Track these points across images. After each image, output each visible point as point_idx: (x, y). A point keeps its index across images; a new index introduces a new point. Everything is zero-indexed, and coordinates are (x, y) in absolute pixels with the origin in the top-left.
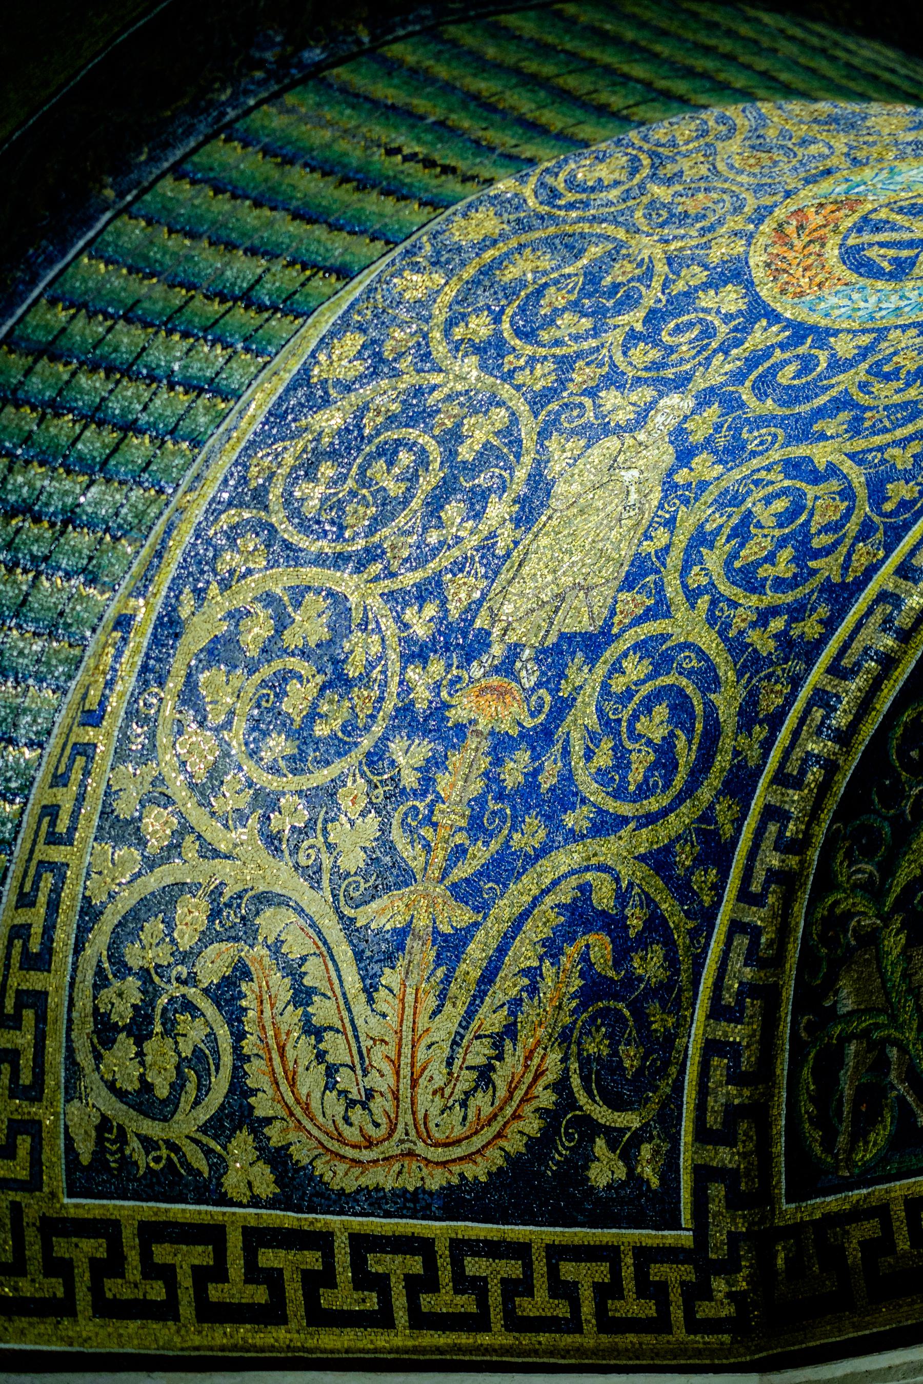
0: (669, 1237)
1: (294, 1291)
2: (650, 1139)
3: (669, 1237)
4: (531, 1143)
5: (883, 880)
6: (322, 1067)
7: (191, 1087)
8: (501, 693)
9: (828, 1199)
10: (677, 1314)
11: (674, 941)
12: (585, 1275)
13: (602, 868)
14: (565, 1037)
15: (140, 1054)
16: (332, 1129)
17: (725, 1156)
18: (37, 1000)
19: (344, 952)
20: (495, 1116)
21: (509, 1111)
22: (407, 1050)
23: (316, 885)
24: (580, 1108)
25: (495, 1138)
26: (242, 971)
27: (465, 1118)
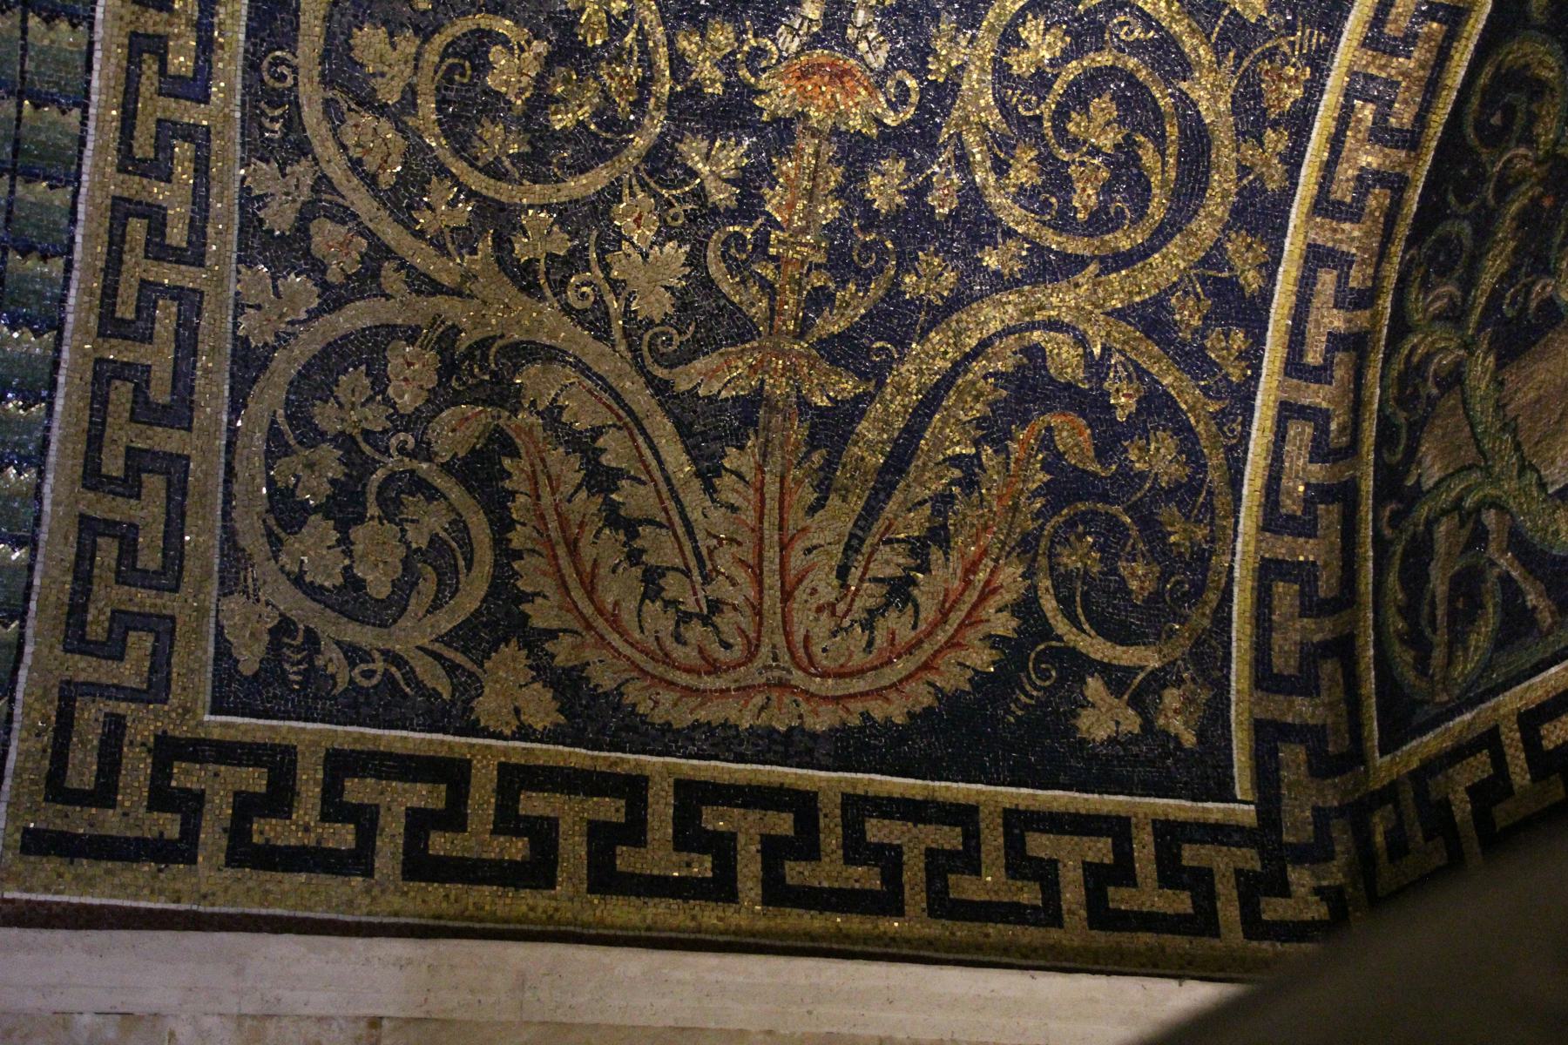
0: (1214, 810)
1: (573, 848)
2: (1180, 682)
3: (1214, 810)
4: (980, 680)
5: (1464, 300)
6: (637, 571)
7: (428, 587)
8: (840, 75)
9: (1425, 739)
10: (1229, 911)
11: (1191, 429)
12: (1073, 857)
13: (1053, 325)
14: (1027, 545)
15: (345, 541)
16: (654, 646)
17: (1302, 709)
18: (175, 467)
19: (663, 428)
20: (919, 643)
21: (941, 637)
22: (772, 554)
23: (603, 335)
24: (1059, 638)
25: (919, 669)
26: (502, 443)
27: (870, 643)
